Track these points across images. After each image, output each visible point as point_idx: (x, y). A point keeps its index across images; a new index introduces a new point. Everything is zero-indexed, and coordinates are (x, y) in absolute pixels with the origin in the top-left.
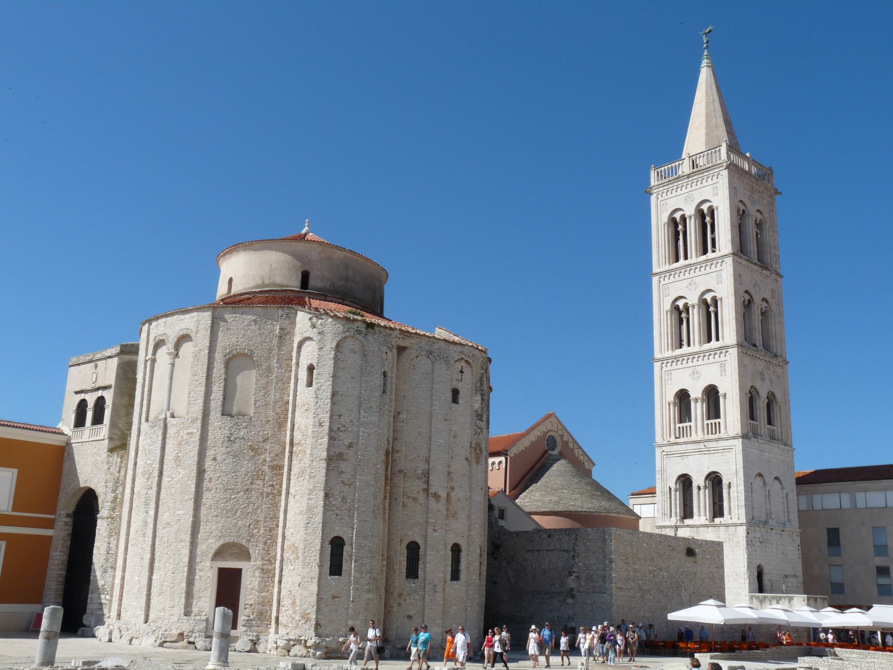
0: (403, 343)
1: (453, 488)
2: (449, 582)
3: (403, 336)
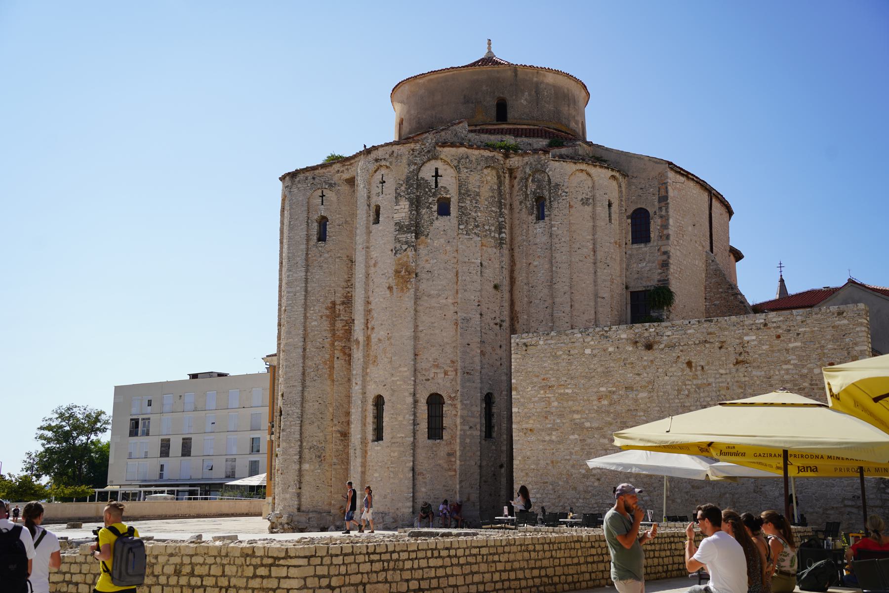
0: (346, 176)
1: (373, 329)
2: (370, 444)
3: (346, 167)
